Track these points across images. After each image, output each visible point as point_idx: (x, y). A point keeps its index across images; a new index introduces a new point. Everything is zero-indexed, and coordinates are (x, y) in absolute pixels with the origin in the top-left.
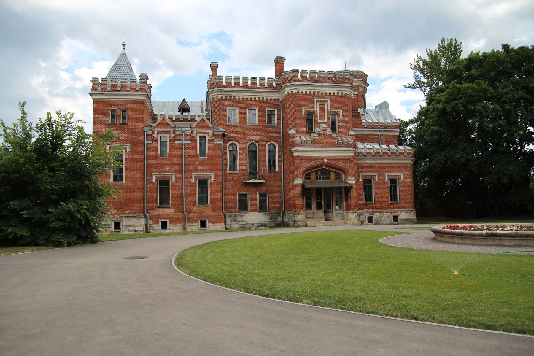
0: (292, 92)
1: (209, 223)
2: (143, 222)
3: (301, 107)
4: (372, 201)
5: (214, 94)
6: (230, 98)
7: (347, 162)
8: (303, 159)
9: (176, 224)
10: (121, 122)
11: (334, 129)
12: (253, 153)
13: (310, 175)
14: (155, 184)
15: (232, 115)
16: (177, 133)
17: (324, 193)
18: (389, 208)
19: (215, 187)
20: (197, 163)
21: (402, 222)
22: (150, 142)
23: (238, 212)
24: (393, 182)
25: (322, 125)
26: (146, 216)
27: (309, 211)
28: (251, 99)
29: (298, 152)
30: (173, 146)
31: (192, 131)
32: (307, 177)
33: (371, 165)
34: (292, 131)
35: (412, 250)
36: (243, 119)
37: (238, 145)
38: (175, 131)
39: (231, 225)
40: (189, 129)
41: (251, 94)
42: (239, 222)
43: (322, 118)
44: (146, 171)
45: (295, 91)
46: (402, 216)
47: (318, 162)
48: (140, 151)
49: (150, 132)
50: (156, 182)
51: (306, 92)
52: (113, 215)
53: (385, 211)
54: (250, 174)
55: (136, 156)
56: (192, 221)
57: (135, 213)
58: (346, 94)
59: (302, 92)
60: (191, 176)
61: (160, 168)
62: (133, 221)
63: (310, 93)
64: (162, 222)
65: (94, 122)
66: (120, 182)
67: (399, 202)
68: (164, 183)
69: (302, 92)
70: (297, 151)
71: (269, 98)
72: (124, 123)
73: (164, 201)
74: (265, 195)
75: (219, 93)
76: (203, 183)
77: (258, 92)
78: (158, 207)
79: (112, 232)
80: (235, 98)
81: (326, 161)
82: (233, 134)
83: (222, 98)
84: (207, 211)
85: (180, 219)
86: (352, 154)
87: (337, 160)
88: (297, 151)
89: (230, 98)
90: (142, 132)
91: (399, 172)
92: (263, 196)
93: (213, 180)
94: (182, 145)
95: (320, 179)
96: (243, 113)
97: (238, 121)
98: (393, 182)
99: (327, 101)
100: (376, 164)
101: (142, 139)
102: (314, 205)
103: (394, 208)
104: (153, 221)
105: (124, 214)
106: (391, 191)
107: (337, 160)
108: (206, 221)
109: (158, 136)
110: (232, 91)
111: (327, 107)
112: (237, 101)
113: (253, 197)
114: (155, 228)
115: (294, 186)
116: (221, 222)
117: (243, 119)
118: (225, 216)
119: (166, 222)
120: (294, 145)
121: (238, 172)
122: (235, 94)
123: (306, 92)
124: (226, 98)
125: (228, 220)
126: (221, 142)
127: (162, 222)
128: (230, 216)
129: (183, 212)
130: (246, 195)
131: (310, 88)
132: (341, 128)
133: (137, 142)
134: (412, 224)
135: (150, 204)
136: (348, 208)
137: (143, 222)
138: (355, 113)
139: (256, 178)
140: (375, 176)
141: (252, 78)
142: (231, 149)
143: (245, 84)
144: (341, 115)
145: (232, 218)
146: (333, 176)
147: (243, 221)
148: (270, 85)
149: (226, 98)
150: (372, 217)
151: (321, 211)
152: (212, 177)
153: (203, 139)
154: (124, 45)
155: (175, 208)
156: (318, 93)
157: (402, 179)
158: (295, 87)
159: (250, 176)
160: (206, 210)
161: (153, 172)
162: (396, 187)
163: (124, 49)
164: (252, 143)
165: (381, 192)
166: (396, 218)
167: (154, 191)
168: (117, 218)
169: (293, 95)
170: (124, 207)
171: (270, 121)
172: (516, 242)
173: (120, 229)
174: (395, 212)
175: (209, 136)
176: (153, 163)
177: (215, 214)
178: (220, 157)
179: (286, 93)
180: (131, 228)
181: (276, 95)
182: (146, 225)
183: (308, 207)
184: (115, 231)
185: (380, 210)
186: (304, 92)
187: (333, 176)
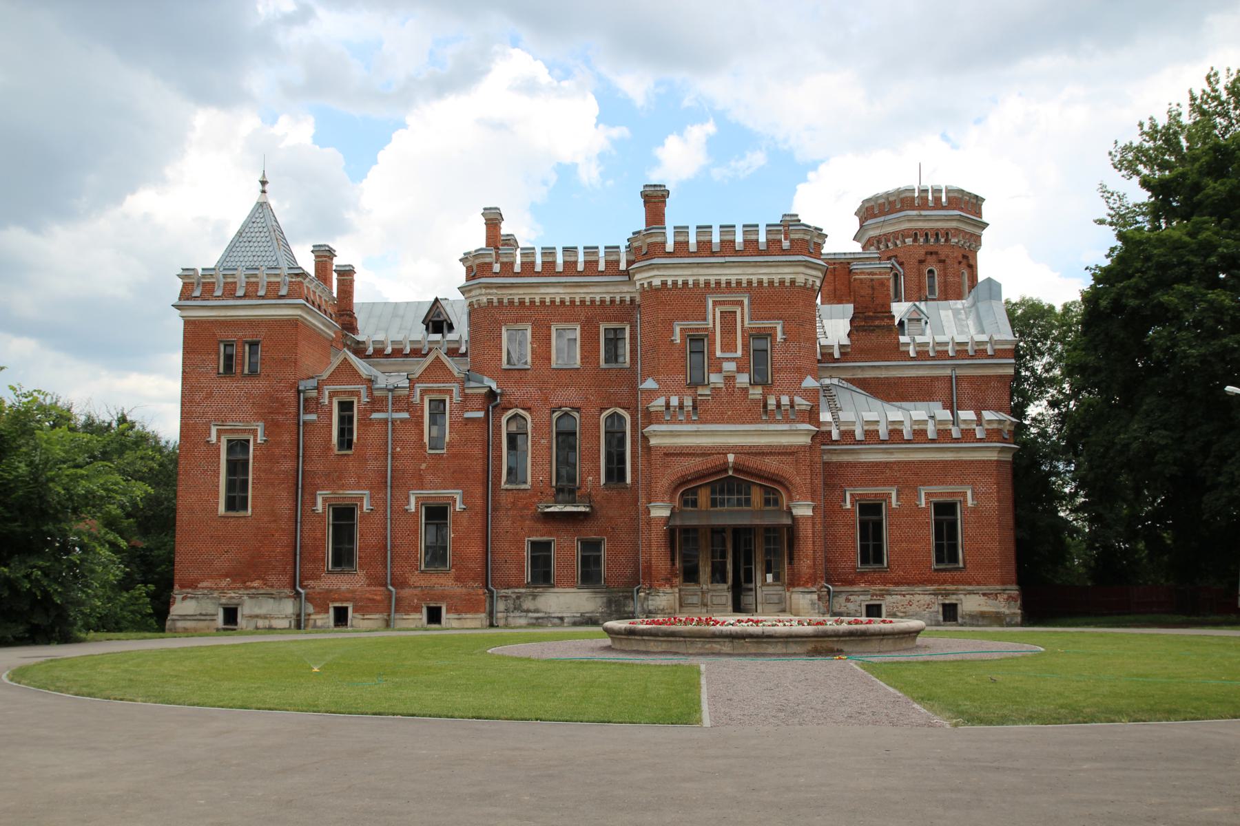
0: (650, 284)
1: (448, 612)
2: (289, 607)
3: (671, 322)
4: (881, 562)
5: (473, 293)
6: (511, 302)
7: (790, 459)
8: (671, 454)
9: (371, 613)
10: (246, 371)
11: (760, 380)
12: (566, 439)
13: (696, 494)
14: (321, 517)
15: (516, 344)
16: (376, 393)
17: (732, 540)
18: (929, 582)
19: (465, 523)
20: (423, 466)
21: (967, 620)
22: (313, 417)
23: (527, 586)
24: (945, 510)
25: (728, 366)
26: (298, 594)
27: (692, 587)
28: (562, 302)
29: (662, 436)
30: (365, 425)
31: (411, 388)
32: (689, 500)
33: (877, 464)
34: (650, 384)
35: (529, 659)
36: (542, 354)
37: (529, 420)
38: (370, 390)
39: (506, 618)
40: (406, 383)
41: (561, 290)
42: (528, 611)
43: (728, 346)
44: (301, 486)
45: (657, 282)
46: (970, 603)
47: (715, 461)
48: (287, 438)
49: (314, 394)
50: (417, 511)
51: (685, 283)
52: (223, 591)
53: (918, 589)
54: (560, 490)
55: (277, 451)
56: (403, 606)
57: (272, 586)
58: (793, 282)
59: (675, 283)
60: (408, 498)
61: (335, 478)
62: (267, 607)
63: (696, 284)
64: (335, 608)
65: (184, 372)
66: (241, 513)
67: (961, 565)
68: (344, 515)
69: (675, 283)
70: (656, 434)
71: (608, 299)
72: (253, 373)
73: (343, 558)
74: (596, 545)
75: (483, 291)
76: (437, 513)
77: (578, 285)
78: (329, 572)
79: (218, 630)
80: (522, 303)
81: (731, 458)
82: (516, 392)
83: (490, 302)
84: (444, 583)
85: (379, 602)
86: (806, 440)
87: (764, 454)
88: (656, 434)
89: (511, 302)
90: (291, 394)
91: (962, 483)
92: (591, 546)
93: (459, 506)
94: (386, 421)
95: (722, 504)
96: (542, 339)
97: (529, 360)
98: (945, 510)
99: (741, 303)
100: (895, 463)
101: (293, 410)
102: (705, 572)
103: (945, 582)
104: (315, 606)
105: (247, 588)
106: (939, 536)
107: (764, 454)
108: (440, 608)
109: (330, 402)
110: (512, 286)
111: (744, 320)
112: (529, 308)
113: (566, 551)
114: (319, 623)
115: (649, 521)
116: (477, 612)
117: (542, 354)
118: (492, 597)
119: (346, 608)
120: (650, 418)
121: (528, 486)
122: (521, 291)
123: (685, 283)
124: (500, 302)
125: (500, 606)
126: (481, 414)
127: (335, 608)
128: (506, 597)
129: (385, 585)
130: (547, 545)
131: (696, 271)
132: (779, 371)
133: (281, 418)
134: (1002, 626)
135: (309, 566)
136: (793, 582)
137: (289, 607)
138: (882, 319)
139: (573, 502)
141: (565, 250)
142: (513, 428)
143: (549, 267)
144: (780, 336)
145: (510, 602)
146: (757, 496)
147: (537, 611)
148: (612, 265)
149: (500, 302)
150: (879, 606)
151: (725, 586)
152: (458, 498)
153: (438, 408)
154: (263, 183)
155: (369, 576)
157: (970, 503)
158: (655, 272)
159: (560, 497)
160: (441, 581)
161: (318, 489)
162: (953, 525)
163: (264, 192)
164: (566, 413)
165: (908, 538)
166: (950, 613)
167: (319, 535)
168: (230, 597)
169: (651, 292)
170: (247, 572)
171: (613, 356)
172: (664, 647)
173: (236, 623)
174: (947, 594)
175: (451, 398)
176: (318, 466)
177: (464, 590)
178: (477, 451)
179: (638, 286)
180: (261, 623)
181: (625, 289)
182: (299, 615)
183: (691, 575)
184: (225, 629)
185: (904, 588)
186: (680, 283)
187: (757, 496)
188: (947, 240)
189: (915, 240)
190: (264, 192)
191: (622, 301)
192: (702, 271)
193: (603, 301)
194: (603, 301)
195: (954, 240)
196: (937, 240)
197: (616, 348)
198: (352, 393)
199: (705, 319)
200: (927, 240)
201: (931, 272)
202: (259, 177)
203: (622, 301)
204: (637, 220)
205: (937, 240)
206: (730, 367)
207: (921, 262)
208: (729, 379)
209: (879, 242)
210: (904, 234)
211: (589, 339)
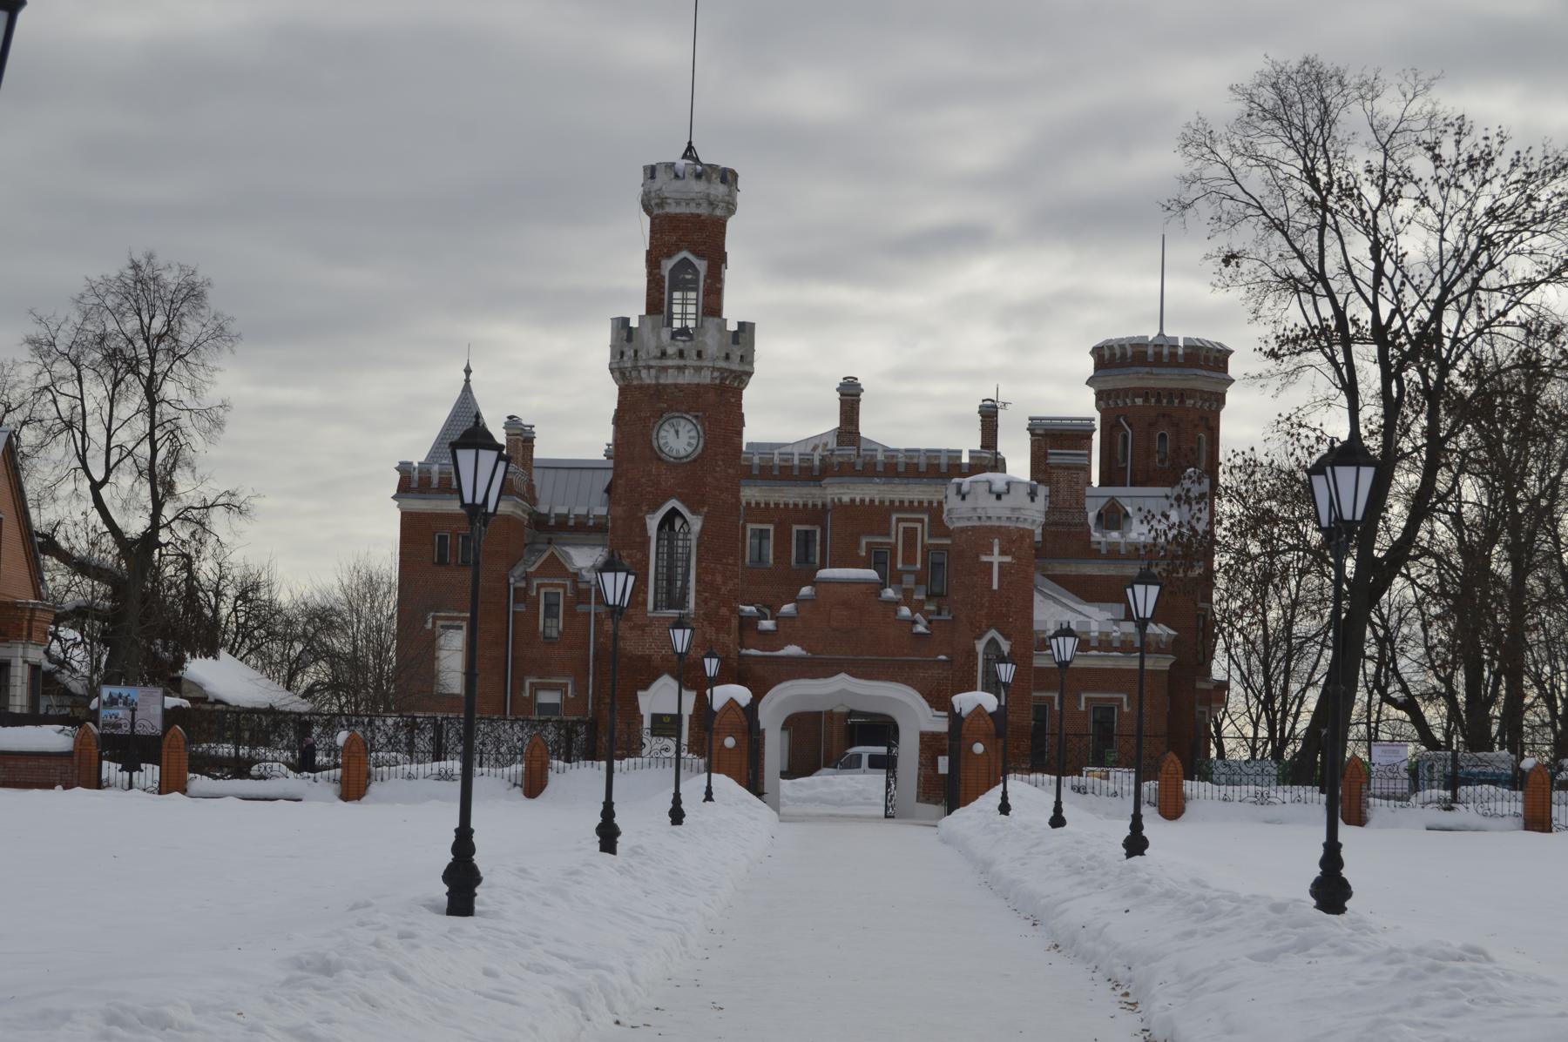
43: (909, 559)
45: (846, 499)
51: (872, 501)
99: (922, 521)
111: (923, 538)
123: (872, 501)
140: (1052, 699)
156: (902, 502)
157: (1126, 709)
189: (1146, 400)
191: (815, 505)
193: (796, 505)
194: (796, 505)
195: (1190, 403)
197: (807, 547)
198: (559, 585)
199: (888, 535)
200: (1159, 401)
201: (1163, 436)
203: (815, 505)
209: (1109, 397)
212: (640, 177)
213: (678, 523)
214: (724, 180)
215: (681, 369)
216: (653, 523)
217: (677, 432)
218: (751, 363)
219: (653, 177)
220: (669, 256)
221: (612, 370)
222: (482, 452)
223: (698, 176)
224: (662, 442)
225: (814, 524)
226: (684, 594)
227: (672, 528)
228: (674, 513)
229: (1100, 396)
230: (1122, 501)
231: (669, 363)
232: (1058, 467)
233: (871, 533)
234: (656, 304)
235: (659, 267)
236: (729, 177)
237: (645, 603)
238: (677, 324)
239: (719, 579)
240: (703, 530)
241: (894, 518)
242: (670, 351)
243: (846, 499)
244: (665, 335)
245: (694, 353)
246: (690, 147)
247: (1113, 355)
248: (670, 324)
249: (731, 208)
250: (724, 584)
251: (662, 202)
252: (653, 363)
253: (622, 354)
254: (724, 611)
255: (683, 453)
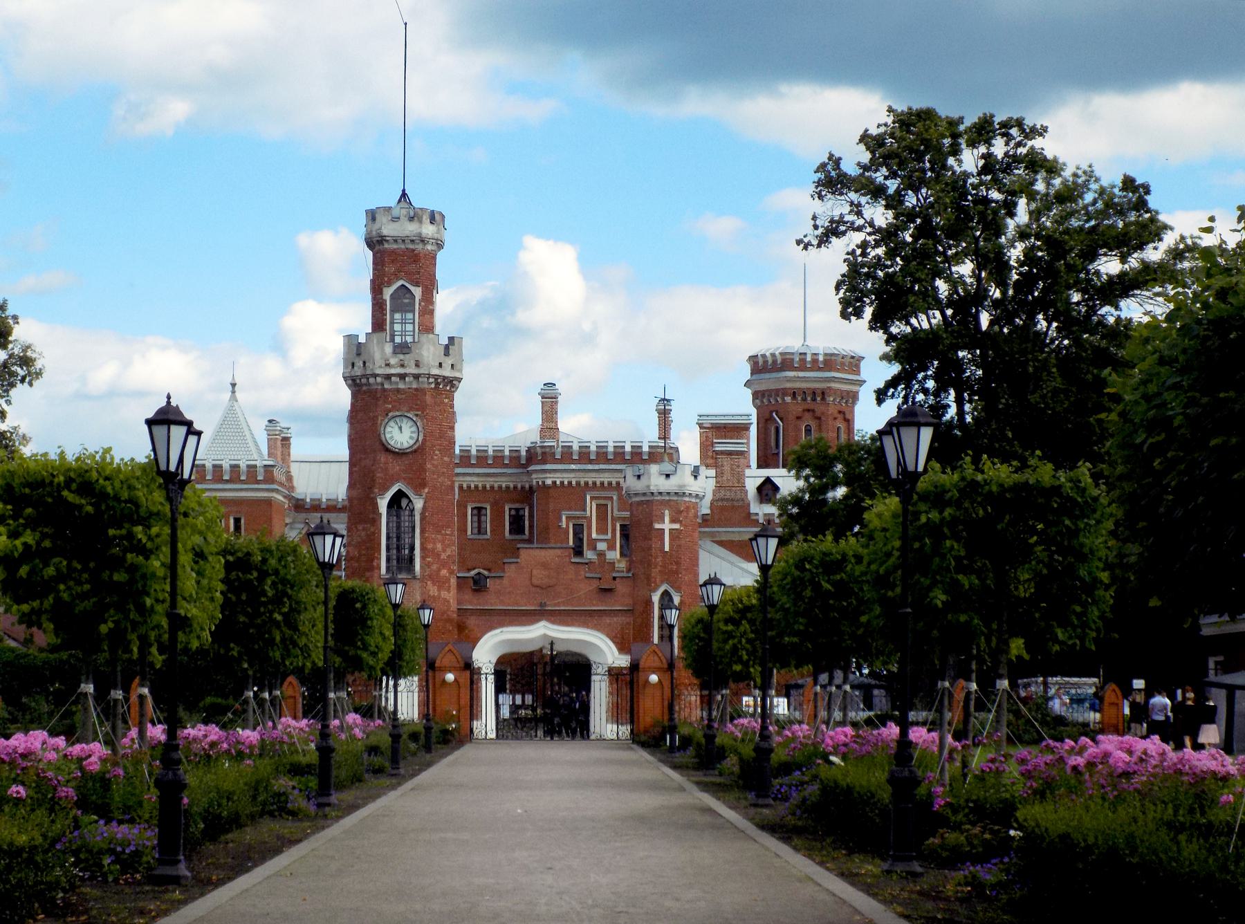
28: (476, 487)
41: (475, 479)
45: (549, 482)
51: (570, 483)
59: (562, 483)
63: (578, 483)
69: (562, 483)
111: (614, 510)
123: (570, 483)
154: (234, 385)
156: (594, 483)
181: (525, 478)
188: (823, 399)
190: (233, 392)
191: (523, 488)
192: (582, 474)
193: (508, 487)
194: (508, 487)
196: (814, 399)
199: (585, 510)
200: (804, 399)
202: (230, 380)
203: (523, 488)
204: (537, 420)
205: (814, 399)
206: (602, 546)
207: (798, 418)
208: (601, 555)
209: (763, 396)
210: (784, 392)
211: (497, 516)
212: (363, 220)
213: (404, 502)
214: (432, 220)
215: (402, 377)
216: (383, 504)
217: (400, 428)
218: (460, 371)
219: (374, 219)
220: (389, 284)
221: (345, 378)
222: (173, 428)
223: (411, 219)
224: (388, 436)
225: (522, 502)
226: (411, 559)
227: (400, 507)
228: (400, 495)
229: (756, 395)
230: (776, 481)
231: (393, 371)
232: (722, 453)
233: (570, 509)
234: (378, 324)
235: (381, 293)
236: (437, 217)
237: (380, 569)
238: (398, 340)
239: (439, 546)
240: (424, 508)
241: (588, 498)
242: (393, 361)
243: (549, 482)
244: (389, 349)
245: (413, 363)
246: (404, 194)
247: (766, 362)
248: (392, 340)
249: (440, 246)
250: (444, 551)
251: (382, 240)
252: (378, 371)
253: (353, 365)
254: (444, 572)
255: (406, 445)
